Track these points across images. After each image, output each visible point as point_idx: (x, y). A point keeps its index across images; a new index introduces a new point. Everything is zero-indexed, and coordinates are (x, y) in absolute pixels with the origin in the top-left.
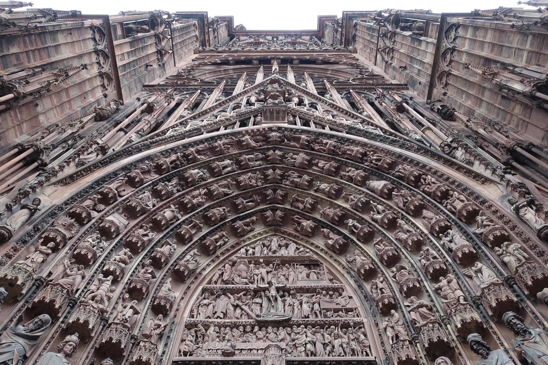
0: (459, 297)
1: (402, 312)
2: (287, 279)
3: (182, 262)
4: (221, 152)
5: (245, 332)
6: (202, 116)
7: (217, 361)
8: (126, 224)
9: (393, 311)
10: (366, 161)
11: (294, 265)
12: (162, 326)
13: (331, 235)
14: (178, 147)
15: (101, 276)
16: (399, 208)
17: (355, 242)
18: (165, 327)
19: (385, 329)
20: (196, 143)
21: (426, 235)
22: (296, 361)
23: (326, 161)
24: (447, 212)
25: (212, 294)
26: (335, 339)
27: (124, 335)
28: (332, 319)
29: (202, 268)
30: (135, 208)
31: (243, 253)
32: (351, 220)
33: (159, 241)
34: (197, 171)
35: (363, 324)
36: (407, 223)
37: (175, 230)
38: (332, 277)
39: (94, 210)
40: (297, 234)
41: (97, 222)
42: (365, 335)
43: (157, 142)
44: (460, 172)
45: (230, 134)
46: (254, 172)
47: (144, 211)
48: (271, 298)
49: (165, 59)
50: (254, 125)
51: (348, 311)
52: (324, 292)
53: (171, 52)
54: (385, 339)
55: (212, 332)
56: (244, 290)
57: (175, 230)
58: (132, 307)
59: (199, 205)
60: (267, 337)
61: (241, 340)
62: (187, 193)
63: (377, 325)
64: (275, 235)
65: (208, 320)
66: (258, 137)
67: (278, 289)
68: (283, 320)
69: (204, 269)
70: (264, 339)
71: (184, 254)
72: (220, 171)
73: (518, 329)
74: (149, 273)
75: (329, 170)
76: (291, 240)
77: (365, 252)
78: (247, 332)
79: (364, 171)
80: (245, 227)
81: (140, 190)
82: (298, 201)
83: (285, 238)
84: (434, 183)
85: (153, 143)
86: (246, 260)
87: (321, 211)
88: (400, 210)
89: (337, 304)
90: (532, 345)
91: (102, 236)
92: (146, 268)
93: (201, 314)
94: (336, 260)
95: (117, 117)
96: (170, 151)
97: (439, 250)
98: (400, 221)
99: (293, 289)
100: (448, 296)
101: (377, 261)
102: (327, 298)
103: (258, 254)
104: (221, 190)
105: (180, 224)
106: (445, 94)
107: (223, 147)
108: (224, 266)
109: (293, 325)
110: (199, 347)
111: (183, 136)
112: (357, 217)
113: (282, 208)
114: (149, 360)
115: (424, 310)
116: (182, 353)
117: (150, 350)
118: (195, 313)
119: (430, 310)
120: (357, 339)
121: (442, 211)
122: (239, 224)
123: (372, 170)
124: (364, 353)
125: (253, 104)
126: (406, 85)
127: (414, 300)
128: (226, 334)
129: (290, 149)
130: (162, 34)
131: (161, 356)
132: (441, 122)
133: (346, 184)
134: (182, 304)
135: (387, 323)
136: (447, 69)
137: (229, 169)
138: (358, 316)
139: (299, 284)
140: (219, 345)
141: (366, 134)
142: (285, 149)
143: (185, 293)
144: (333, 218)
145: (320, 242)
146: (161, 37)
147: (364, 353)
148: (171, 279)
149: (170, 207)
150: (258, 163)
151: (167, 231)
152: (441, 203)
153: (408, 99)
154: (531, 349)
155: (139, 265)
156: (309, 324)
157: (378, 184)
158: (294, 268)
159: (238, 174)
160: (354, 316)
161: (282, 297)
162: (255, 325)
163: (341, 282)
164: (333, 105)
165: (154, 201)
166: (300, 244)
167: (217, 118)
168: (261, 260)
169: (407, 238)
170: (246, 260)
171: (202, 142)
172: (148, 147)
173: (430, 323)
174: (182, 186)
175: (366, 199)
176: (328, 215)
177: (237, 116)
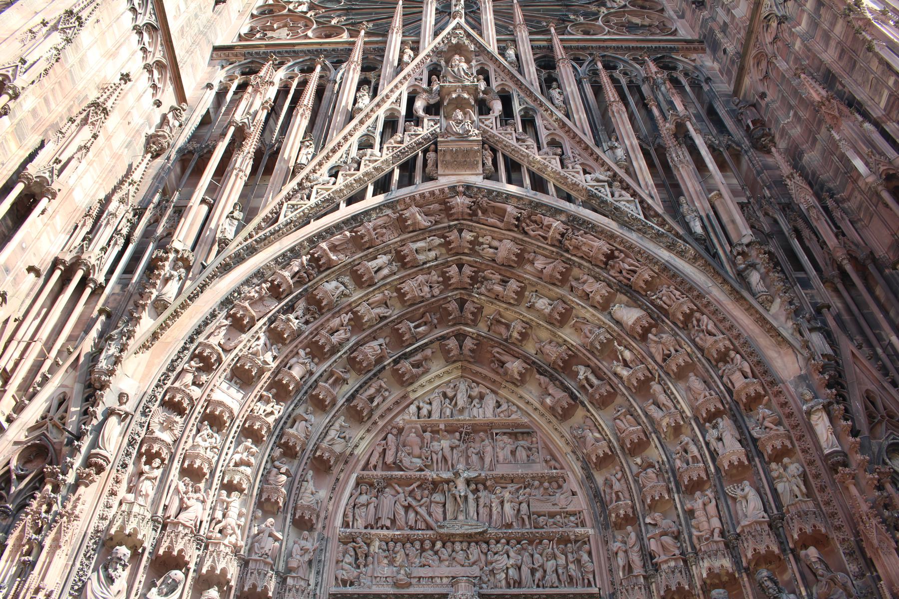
1: (641, 531)
2: (482, 459)
3: (324, 445)
5: (423, 550)
10: (613, 267)
11: (492, 434)
16: (655, 361)
17: (585, 406)
18: (314, 550)
19: (617, 553)
20: (329, 231)
21: (687, 417)
23: (546, 257)
26: (547, 560)
33: (289, 416)
34: (334, 284)
35: (588, 537)
37: (309, 392)
38: (549, 458)
42: (590, 554)
43: (266, 237)
44: (751, 315)
45: (384, 205)
46: (429, 271)
48: (458, 499)
54: (614, 564)
55: (377, 551)
56: (418, 479)
59: (341, 344)
60: (454, 559)
61: (417, 561)
62: (322, 325)
64: (462, 377)
65: (369, 530)
66: (432, 207)
67: (468, 482)
68: (476, 533)
69: (356, 446)
72: (372, 278)
75: (551, 276)
79: (609, 285)
80: (414, 370)
81: (253, 336)
82: (499, 322)
83: (478, 384)
84: (710, 334)
86: (419, 426)
87: (538, 346)
88: (656, 367)
93: (359, 521)
98: (656, 387)
100: (700, 526)
102: (538, 493)
105: (316, 381)
108: (385, 438)
112: (592, 365)
113: (473, 333)
115: (667, 540)
117: (303, 591)
118: (350, 519)
119: (677, 537)
120: (578, 561)
121: (715, 382)
122: (405, 366)
124: (586, 581)
125: (418, 122)
126: (701, 42)
129: (487, 230)
133: (578, 304)
134: (330, 508)
137: (385, 272)
138: (583, 526)
139: (501, 470)
140: (387, 571)
141: (614, 213)
142: (481, 229)
143: (334, 489)
144: (554, 362)
148: (311, 472)
149: (297, 353)
150: (432, 254)
152: (716, 367)
155: (267, 462)
158: (493, 439)
163: (562, 468)
164: (564, 125)
167: (358, 169)
168: (442, 426)
171: (338, 227)
172: (252, 251)
175: (609, 336)
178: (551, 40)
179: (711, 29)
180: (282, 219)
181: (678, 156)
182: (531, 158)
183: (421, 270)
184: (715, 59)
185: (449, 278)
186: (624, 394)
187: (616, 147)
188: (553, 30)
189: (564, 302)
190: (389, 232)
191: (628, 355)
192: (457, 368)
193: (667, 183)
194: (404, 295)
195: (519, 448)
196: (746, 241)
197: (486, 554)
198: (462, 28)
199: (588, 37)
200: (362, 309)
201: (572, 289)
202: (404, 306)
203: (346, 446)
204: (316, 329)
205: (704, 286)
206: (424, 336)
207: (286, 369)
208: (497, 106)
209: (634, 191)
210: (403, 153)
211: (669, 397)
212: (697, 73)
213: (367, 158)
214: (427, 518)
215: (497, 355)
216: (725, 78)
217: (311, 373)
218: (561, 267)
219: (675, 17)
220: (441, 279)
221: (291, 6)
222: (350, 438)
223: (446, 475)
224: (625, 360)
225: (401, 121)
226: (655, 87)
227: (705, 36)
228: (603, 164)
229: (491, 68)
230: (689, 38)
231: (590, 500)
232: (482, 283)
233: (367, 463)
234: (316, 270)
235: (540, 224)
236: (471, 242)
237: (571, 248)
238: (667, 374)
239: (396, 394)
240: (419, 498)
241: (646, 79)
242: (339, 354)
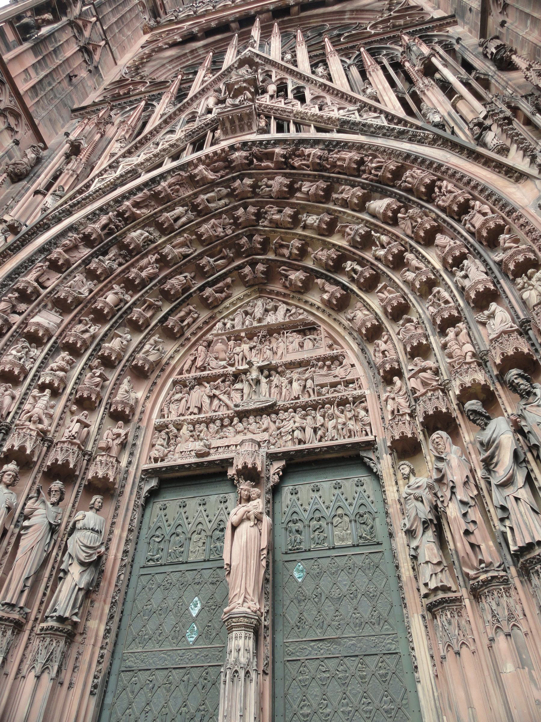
0: (466, 353)
2: (275, 353)
3: (141, 355)
4: (168, 198)
5: (222, 426)
6: (140, 147)
7: (190, 464)
8: (59, 321)
9: (396, 379)
10: (364, 172)
11: (283, 333)
12: (123, 435)
13: (328, 287)
14: (108, 204)
15: (35, 392)
18: (126, 435)
19: (386, 401)
20: (132, 193)
22: (280, 453)
23: (311, 182)
24: (465, 234)
25: (185, 386)
27: (71, 454)
28: (327, 396)
29: (168, 357)
30: (65, 299)
33: (105, 335)
34: (139, 232)
35: (365, 397)
36: (418, 258)
37: (125, 316)
39: (14, 312)
40: (287, 292)
41: (19, 327)
42: (367, 411)
43: (79, 202)
44: (489, 167)
45: (176, 168)
46: (218, 216)
47: (78, 301)
48: (251, 382)
49: (96, 57)
50: (212, 144)
51: (348, 383)
52: (320, 363)
53: (103, 43)
56: (222, 375)
57: (125, 316)
58: (78, 421)
59: (151, 278)
63: (379, 397)
64: (260, 297)
66: (216, 164)
68: (266, 407)
69: (172, 358)
70: (246, 431)
71: (142, 344)
73: (521, 390)
74: (98, 377)
75: (316, 195)
76: (280, 301)
77: (368, 304)
78: (226, 426)
79: (363, 188)
80: (217, 295)
81: (69, 275)
83: (272, 299)
84: (450, 192)
85: (74, 205)
86: (224, 337)
87: (312, 256)
88: (407, 240)
89: (334, 377)
90: (535, 409)
91: (30, 344)
92: (93, 371)
93: (173, 412)
94: (335, 319)
96: (97, 212)
97: (452, 292)
98: (409, 256)
99: (281, 366)
100: (453, 354)
102: (324, 371)
104: (177, 251)
106: (503, 24)
107: (169, 190)
108: (197, 350)
109: (279, 410)
110: (170, 451)
111: (114, 186)
112: (357, 257)
113: (263, 260)
114: (107, 475)
116: (152, 460)
118: (166, 412)
120: (356, 418)
121: (459, 233)
122: (209, 291)
123: (372, 185)
124: (364, 432)
126: (453, 16)
127: (418, 362)
128: (201, 432)
129: (262, 174)
130: (80, 19)
131: (127, 467)
132: (496, 77)
133: (340, 212)
135: (388, 394)
137: (184, 219)
142: (257, 174)
143: (150, 391)
144: (327, 264)
145: (314, 298)
146: (80, 23)
148: (129, 378)
150: (223, 202)
151: (114, 320)
152: (459, 221)
153: (454, 41)
154: (532, 414)
156: (298, 407)
159: (197, 224)
160: (355, 389)
162: (234, 417)
163: (342, 348)
165: (90, 284)
168: (243, 334)
169: (414, 280)
171: (139, 189)
172: (69, 213)
173: (430, 390)
174: (124, 257)
176: (320, 259)
180: (92, 188)
182: (294, 112)
185: (238, 218)
192: (254, 291)
194: (201, 235)
197: (275, 422)
207: (102, 299)
210: (194, 133)
215: (283, 272)
218: (323, 184)
220: (232, 221)
227: (455, 10)
233: (182, 370)
234: (123, 222)
235: (302, 155)
236: (251, 186)
237: (329, 166)
238: (418, 243)
242: (150, 286)
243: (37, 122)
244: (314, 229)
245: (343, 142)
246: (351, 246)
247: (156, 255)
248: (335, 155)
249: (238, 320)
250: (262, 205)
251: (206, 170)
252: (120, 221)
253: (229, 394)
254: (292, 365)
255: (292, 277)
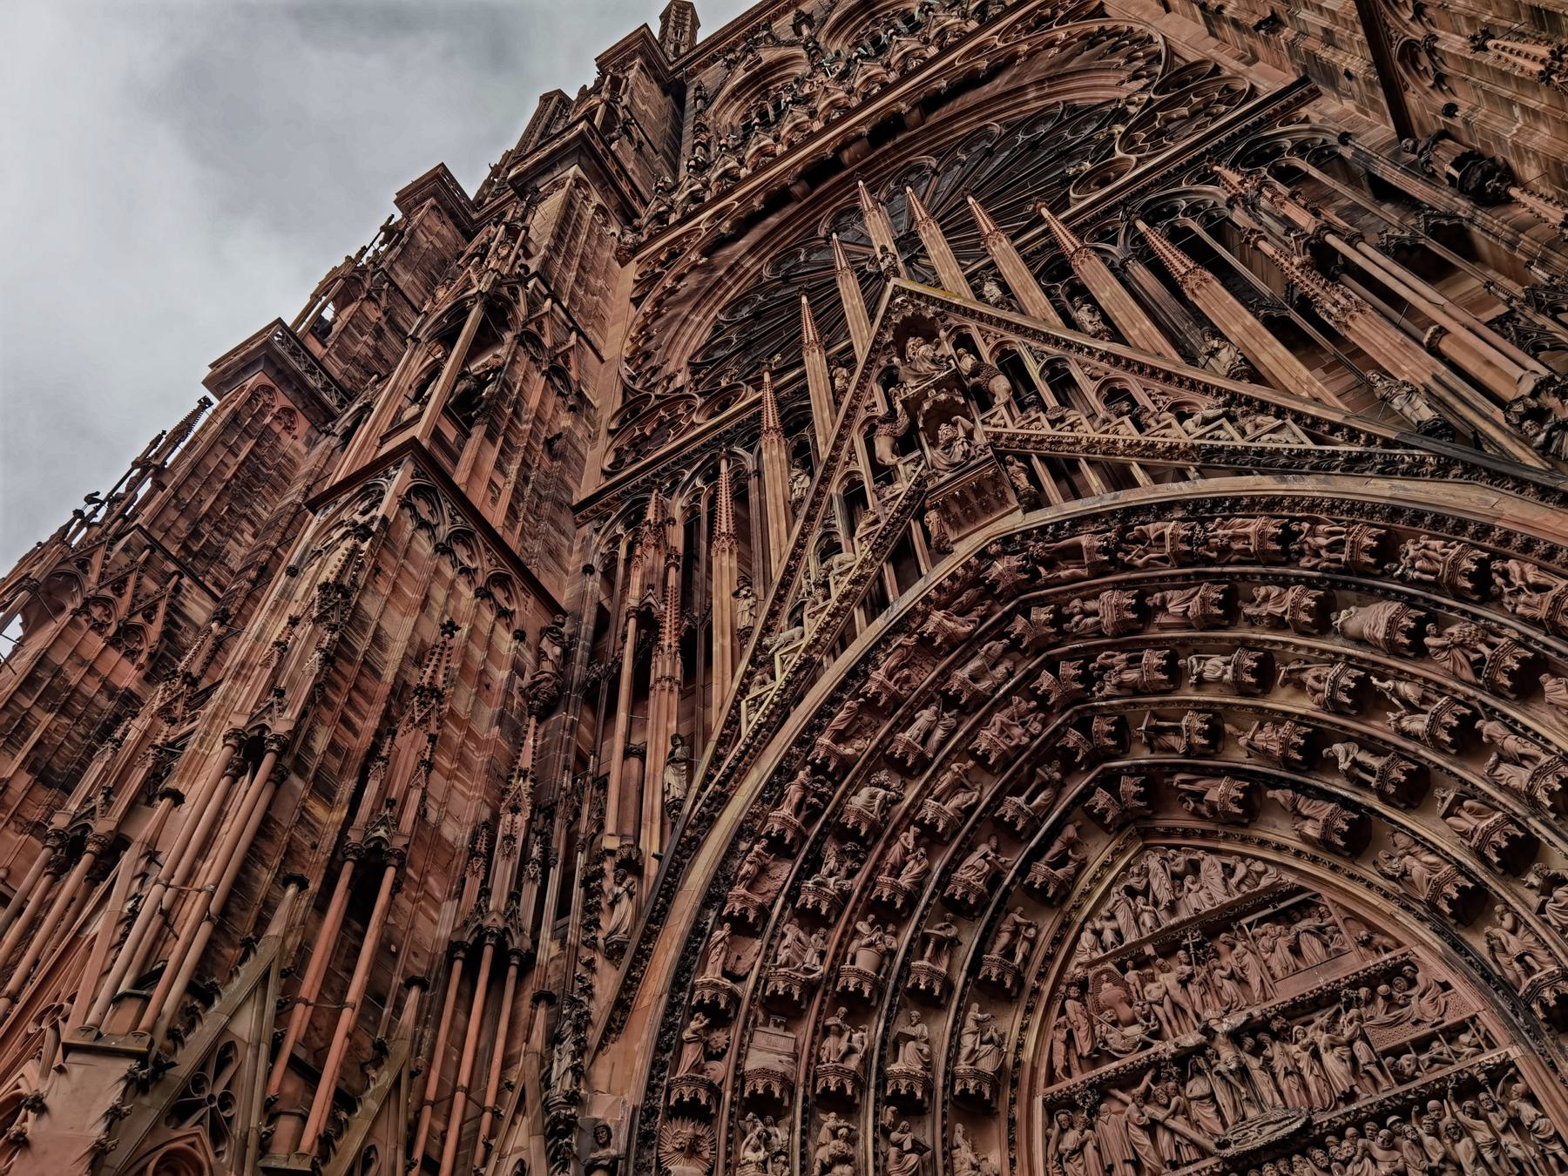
2: (1243, 982)
3: (963, 1066)
10: (1301, 553)
11: (1240, 928)
17: (1381, 815)
20: (824, 712)
26: (1454, 1142)
31: (1094, 949)
32: (1339, 748)
33: (884, 1042)
34: (865, 792)
35: (1512, 1064)
37: (901, 986)
38: (1363, 933)
43: (732, 769)
45: (888, 633)
46: (1006, 700)
47: (810, 988)
48: (1231, 1078)
51: (1452, 1033)
52: (1363, 992)
59: (919, 884)
62: (876, 868)
64: (1146, 847)
66: (963, 598)
68: (1291, 1135)
69: (1020, 1046)
71: (956, 1034)
72: (921, 756)
74: (909, 1152)
80: (1059, 873)
81: (773, 936)
83: (1178, 847)
85: (727, 777)
86: (1110, 965)
87: (1242, 742)
88: (1471, 692)
92: (894, 1136)
95: (576, 672)
98: (1489, 728)
99: (1275, 1017)
101: (1471, 863)
102: (1379, 1012)
103: (1131, 938)
106: (1450, 110)
108: (1063, 1011)
111: (781, 712)
113: (1128, 767)
120: (1515, 1123)
122: (1040, 871)
124: (1552, 1160)
126: (1303, 81)
129: (1066, 592)
133: (1275, 643)
136: (1418, 32)
137: (939, 734)
138: (1492, 1046)
139: (1287, 992)
141: (1265, 462)
143: (1012, 1143)
145: (1281, 831)
147: (1552, 1160)
148: (959, 1127)
149: (856, 932)
150: (1001, 670)
153: (1333, 140)
155: (875, 1141)
156: (1366, 1120)
157: (1372, 619)
159: (967, 734)
161: (1257, 1051)
163: (1399, 945)
164: (1117, 360)
166: (1230, 853)
167: (827, 597)
168: (1149, 950)
169: (1531, 788)
170: (1110, 965)
171: (833, 700)
172: (721, 800)
174: (854, 855)
177: (873, 551)
178: (1048, 232)
179: (1307, 52)
180: (746, 730)
181: (1336, 303)
182: (1084, 442)
183: (995, 704)
184: (1342, 95)
185: (1047, 694)
186: (1439, 767)
187: (1217, 350)
188: (1045, 213)
189: (1252, 649)
190: (916, 670)
191: (1406, 689)
192: (1130, 837)
193: (1342, 355)
194: (986, 756)
195: (1303, 937)
196: (1527, 387)
198: (904, 291)
199: (1108, 189)
200: (929, 810)
201: (1252, 621)
202: (995, 775)
203: (1001, 1053)
204: (870, 878)
205: (1485, 509)
206: (1049, 808)
207: (847, 966)
208: (1001, 385)
209: (1279, 407)
210: (885, 538)
211: (1526, 737)
212: (1320, 137)
213: (836, 571)
214: (1193, 1134)
216: (1373, 117)
217: (892, 954)
219: (1242, 67)
220: (1034, 703)
221: (659, 391)
222: (1002, 1036)
223: (1191, 1039)
224: (1405, 702)
225: (868, 485)
226: (1251, 206)
227: (1305, 68)
228: (1207, 389)
229: (973, 327)
230: (1281, 86)
231: (1480, 988)
232: (1100, 678)
234: (829, 783)
235: (1142, 538)
236: (1051, 623)
237: (1214, 555)
239: (1048, 926)
240: (1165, 1101)
241: (1231, 203)
242: (924, 901)
243: (535, 572)
244: (1225, 684)
245: (1226, 498)
246: (1329, 713)
247: (913, 828)
248: (1220, 532)
249: (1122, 918)
250: (1089, 655)
251: (948, 617)
252: (823, 783)
253: (1186, 1112)
254: (1300, 1010)
255: (1213, 795)
